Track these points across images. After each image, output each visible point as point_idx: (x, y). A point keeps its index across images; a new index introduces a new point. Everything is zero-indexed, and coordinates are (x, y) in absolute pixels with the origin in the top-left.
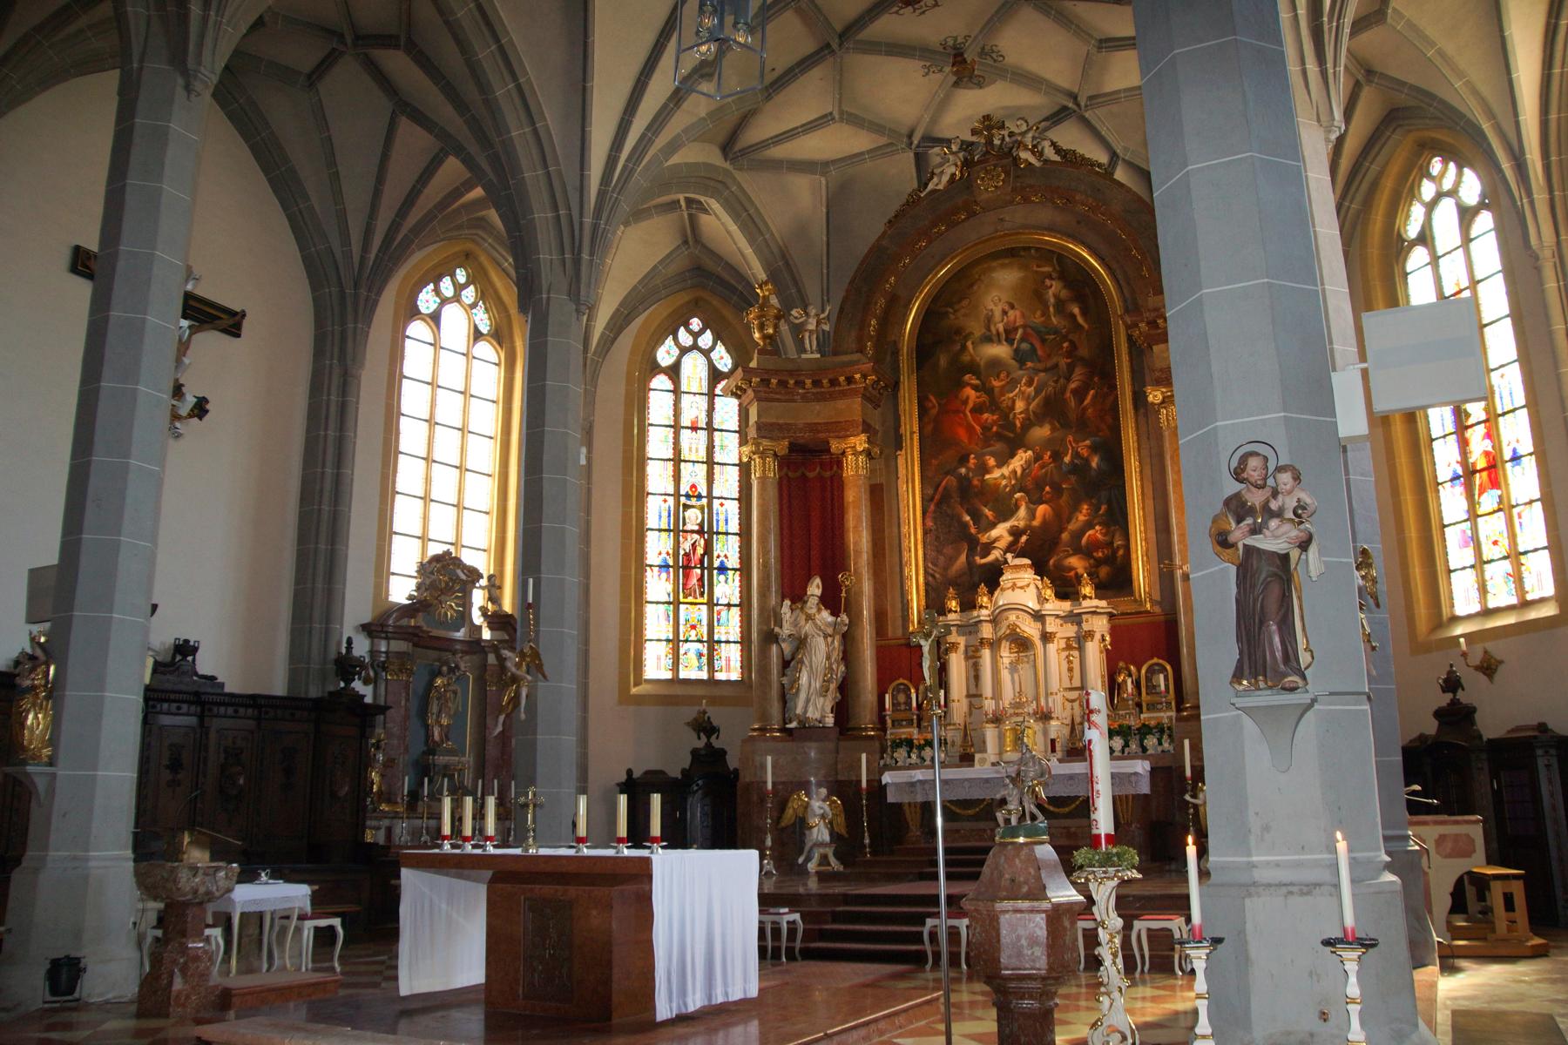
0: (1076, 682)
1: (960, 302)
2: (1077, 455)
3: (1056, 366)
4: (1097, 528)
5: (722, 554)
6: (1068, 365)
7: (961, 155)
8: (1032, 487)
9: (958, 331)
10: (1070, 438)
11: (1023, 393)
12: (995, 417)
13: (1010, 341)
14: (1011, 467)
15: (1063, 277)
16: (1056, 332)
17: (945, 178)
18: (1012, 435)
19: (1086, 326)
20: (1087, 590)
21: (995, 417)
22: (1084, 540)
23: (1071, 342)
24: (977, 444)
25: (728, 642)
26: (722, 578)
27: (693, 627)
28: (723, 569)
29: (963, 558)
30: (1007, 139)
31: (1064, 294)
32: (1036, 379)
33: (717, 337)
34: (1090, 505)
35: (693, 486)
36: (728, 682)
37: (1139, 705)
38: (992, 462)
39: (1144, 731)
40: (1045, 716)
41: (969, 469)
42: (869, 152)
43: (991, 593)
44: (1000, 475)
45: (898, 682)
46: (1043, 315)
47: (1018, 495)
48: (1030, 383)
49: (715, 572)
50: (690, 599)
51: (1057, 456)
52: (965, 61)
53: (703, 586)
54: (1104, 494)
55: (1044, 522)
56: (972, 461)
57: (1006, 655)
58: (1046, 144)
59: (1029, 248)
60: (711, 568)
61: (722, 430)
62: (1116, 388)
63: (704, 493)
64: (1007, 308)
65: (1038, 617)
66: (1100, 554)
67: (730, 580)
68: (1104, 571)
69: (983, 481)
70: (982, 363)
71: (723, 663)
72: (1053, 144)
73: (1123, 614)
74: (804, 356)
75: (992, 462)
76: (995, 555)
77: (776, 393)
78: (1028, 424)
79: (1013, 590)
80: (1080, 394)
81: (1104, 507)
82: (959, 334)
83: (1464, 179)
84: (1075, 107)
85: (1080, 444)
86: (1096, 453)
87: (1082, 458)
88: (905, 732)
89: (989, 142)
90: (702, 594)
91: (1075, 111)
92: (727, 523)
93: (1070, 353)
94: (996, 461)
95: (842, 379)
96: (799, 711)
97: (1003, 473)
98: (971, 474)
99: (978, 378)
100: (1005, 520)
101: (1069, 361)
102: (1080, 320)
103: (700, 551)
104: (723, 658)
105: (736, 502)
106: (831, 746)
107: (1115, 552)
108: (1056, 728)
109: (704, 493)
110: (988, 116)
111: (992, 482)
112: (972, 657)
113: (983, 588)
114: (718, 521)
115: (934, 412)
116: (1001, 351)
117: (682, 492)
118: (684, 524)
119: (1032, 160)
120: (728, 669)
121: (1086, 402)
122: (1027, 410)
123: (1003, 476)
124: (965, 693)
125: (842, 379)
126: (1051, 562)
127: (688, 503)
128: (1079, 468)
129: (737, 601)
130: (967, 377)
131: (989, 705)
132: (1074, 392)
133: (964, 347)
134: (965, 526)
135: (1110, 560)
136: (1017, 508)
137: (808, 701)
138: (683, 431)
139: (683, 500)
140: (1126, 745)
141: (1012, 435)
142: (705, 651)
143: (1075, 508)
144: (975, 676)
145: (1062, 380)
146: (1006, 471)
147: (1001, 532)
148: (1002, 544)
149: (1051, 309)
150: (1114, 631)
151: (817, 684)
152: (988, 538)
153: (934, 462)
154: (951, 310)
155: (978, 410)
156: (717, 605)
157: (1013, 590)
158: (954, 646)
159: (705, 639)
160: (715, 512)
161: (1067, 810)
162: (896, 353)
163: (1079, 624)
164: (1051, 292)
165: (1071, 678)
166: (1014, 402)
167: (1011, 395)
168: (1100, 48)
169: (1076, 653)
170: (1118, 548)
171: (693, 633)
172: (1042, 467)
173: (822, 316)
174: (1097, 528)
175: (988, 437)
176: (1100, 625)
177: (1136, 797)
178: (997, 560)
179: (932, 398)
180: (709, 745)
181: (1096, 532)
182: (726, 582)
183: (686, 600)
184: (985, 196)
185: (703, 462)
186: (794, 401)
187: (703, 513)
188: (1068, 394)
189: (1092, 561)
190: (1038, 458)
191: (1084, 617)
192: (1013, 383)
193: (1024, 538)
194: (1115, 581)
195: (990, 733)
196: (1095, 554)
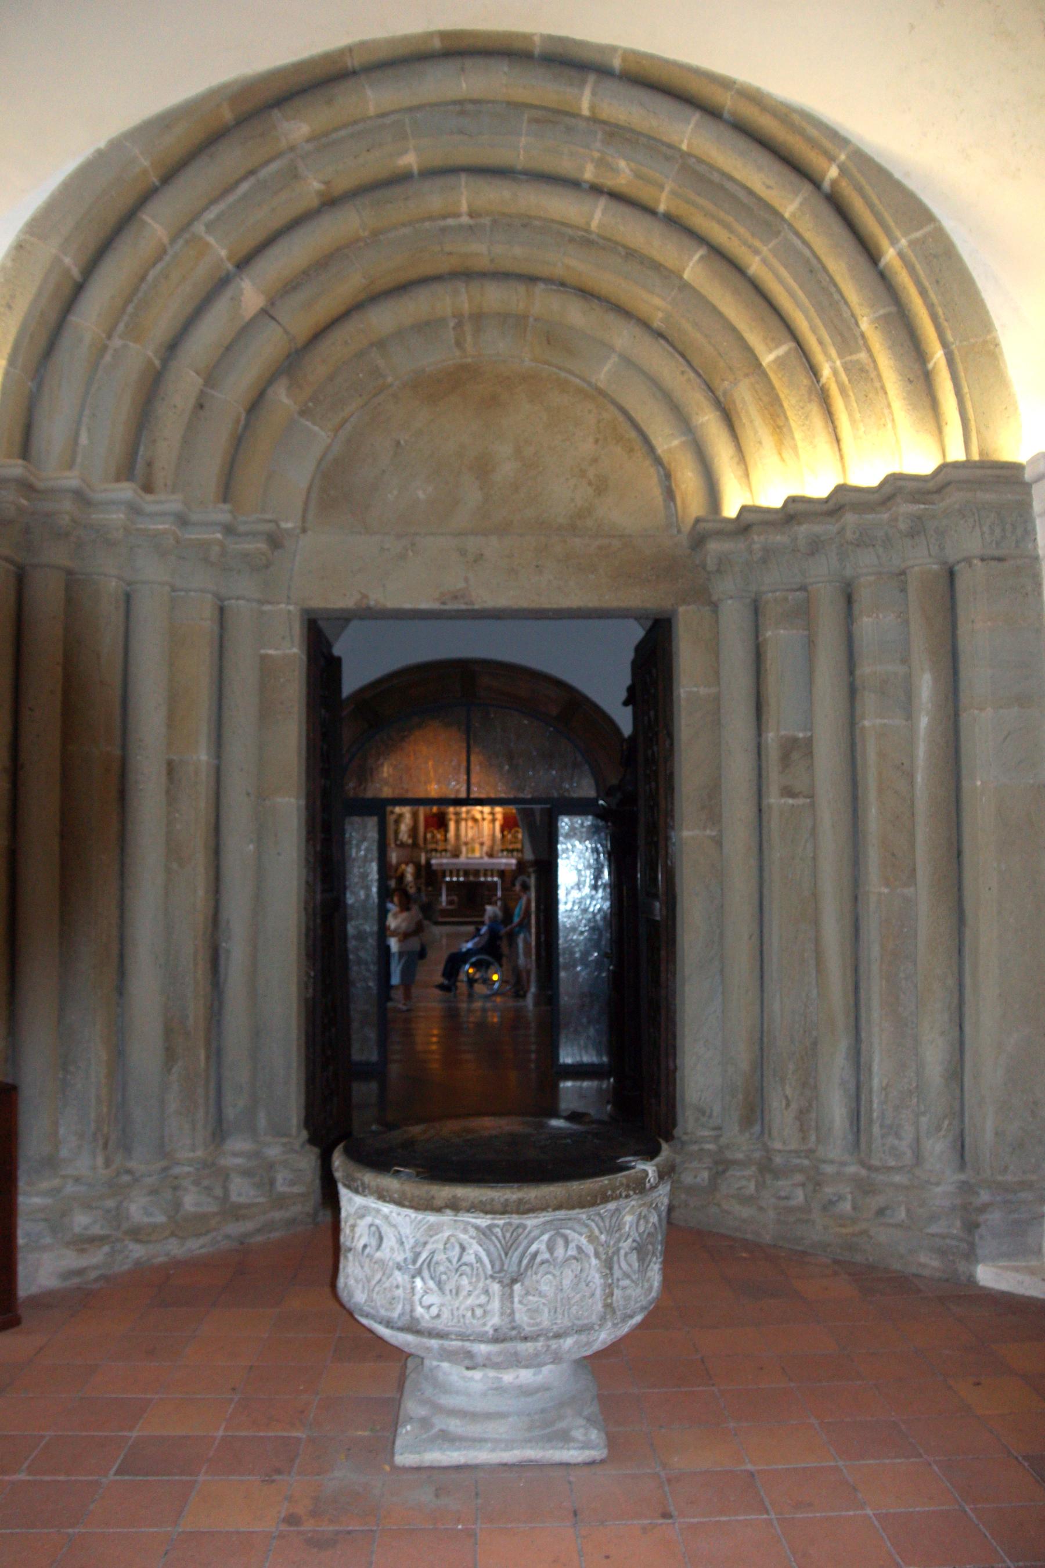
0: (491, 832)
39: (512, 851)
40: (482, 844)
57: (470, 823)
88: (433, 846)
108: (485, 848)
112: (458, 822)
131: (463, 839)
144: (457, 829)
158: (450, 820)
195: (464, 849)
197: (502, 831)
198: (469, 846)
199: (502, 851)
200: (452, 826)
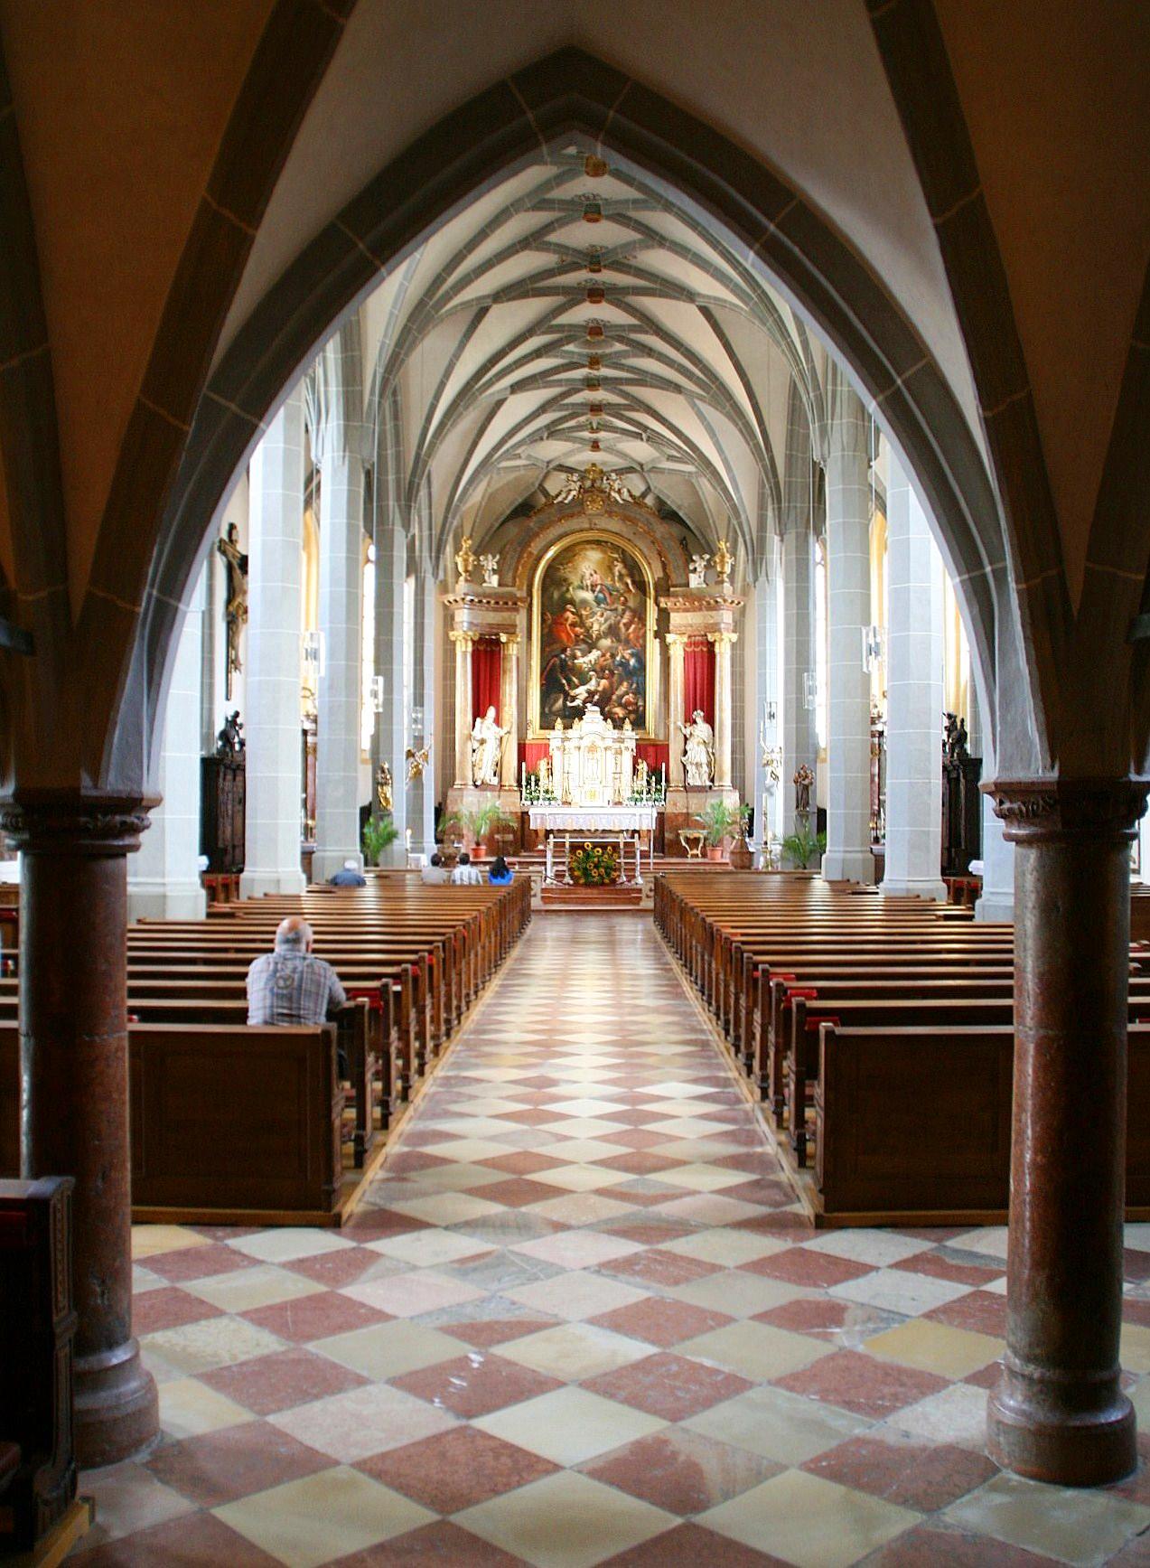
1: (570, 562)
3: (616, 609)
7: (579, 483)
8: (600, 671)
9: (565, 580)
10: (620, 648)
13: (593, 591)
15: (624, 562)
16: (618, 591)
17: (570, 497)
20: (627, 726)
22: (624, 700)
29: (561, 701)
31: (624, 571)
38: (579, 654)
42: (524, 466)
44: (585, 661)
47: (592, 673)
51: (613, 656)
54: (635, 679)
55: (604, 689)
56: (568, 652)
58: (625, 490)
59: (606, 542)
68: (632, 716)
70: (577, 600)
72: (629, 491)
76: (578, 702)
78: (599, 638)
80: (627, 626)
81: (634, 686)
82: (564, 582)
84: (639, 469)
93: (624, 604)
95: (510, 603)
97: (585, 661)
99: (575, 606)
100: (583, 683)
102: (631, 587)
107: (638, 708)
115: (549, 622)
116: (588, 596)
119: (618, 498)
122: (599, 630)
125: (510, 603)
128: (624, 664)
130: (569, 606)
132: (625, 624)
133: (568, 590)
135: (635, 711)
143: (621, 683)
146: (586, 659)
147: (581, 692)
150: (638, 746)
153: (547, 649)
155: (573, 625)
164: (617, 569)
168: (668, 459)
175: (577, 641)
176: (632, 745)
181: (630, 697)
184: (590, 512)
188: (621, 625)
190: (603, 655)
192: (594, 614)
193: (596, 697)
194: (639, 723)
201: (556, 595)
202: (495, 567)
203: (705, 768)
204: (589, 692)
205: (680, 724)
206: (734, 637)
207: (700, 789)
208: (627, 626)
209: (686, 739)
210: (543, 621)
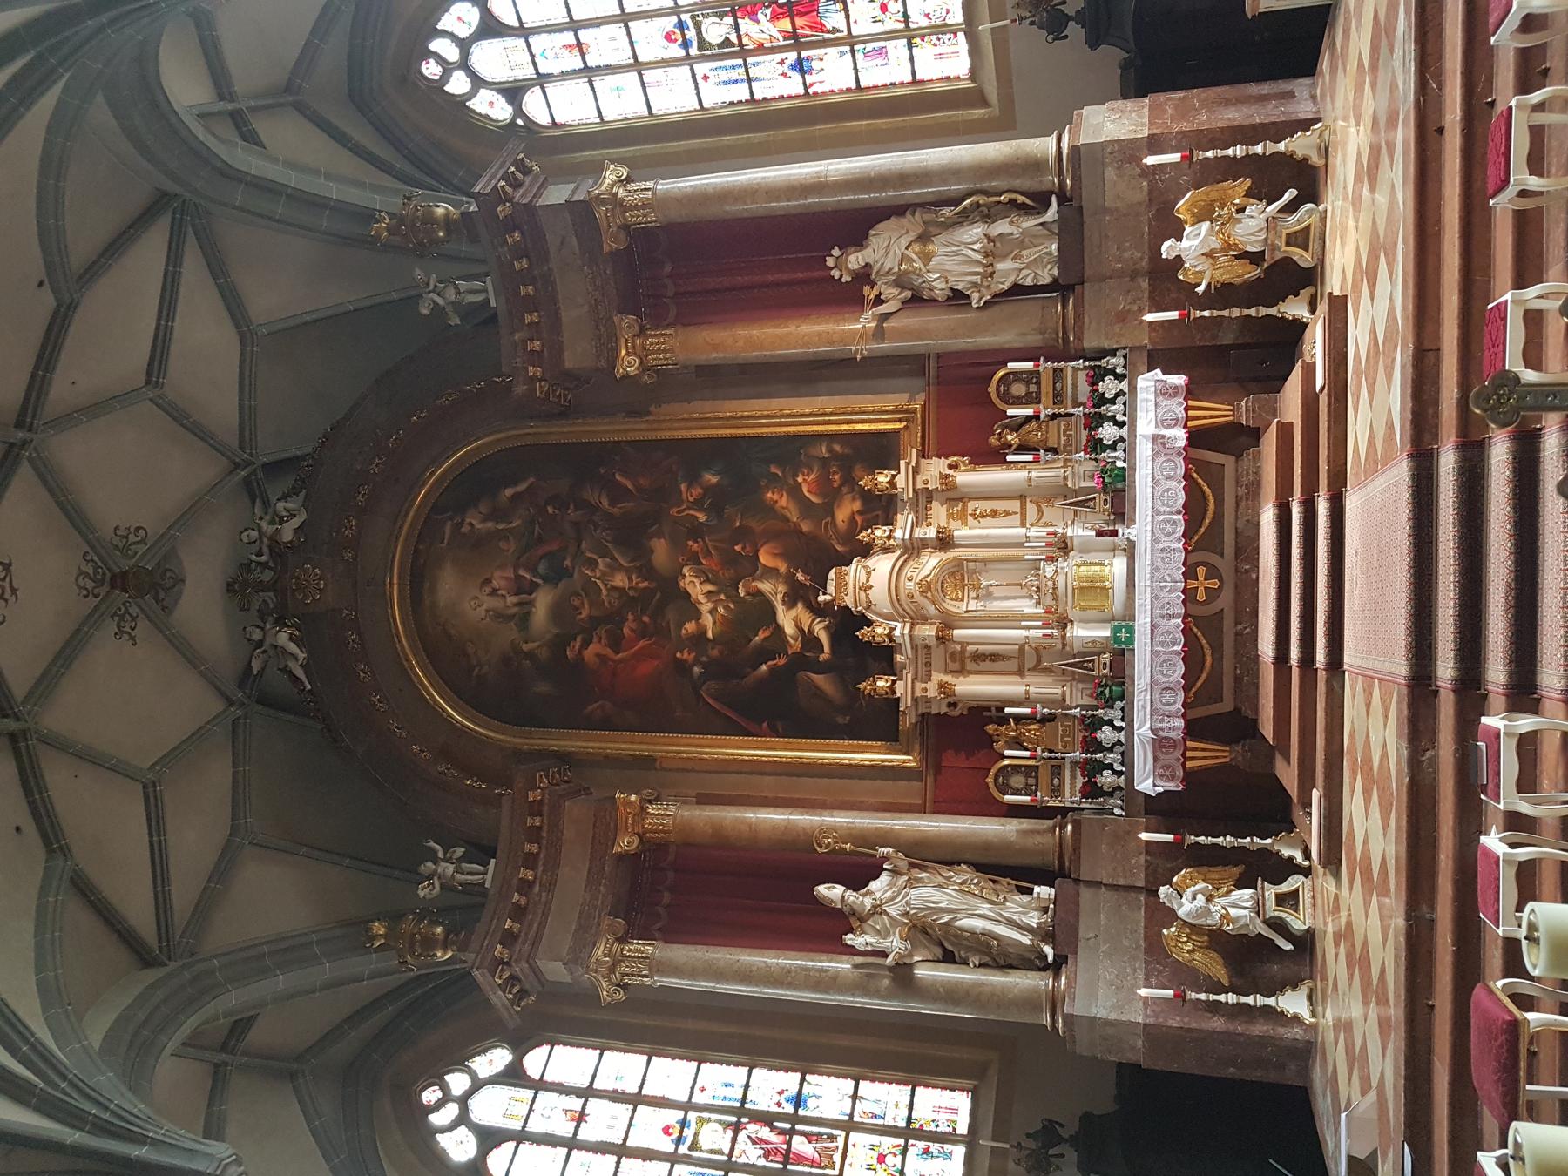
0: (1014, 505)
2: (698, 504)
4: (800, 479)
5: (777, 1098)
6: (576, 509)
10: (674, 511)
11: (604, 574)
12: (630, 617)
13: (534, 587)
14: (702, 599)
17: (293, 647)
18: (658, 595)
19: (532, 480)
20: (883, 478)
21: (630, 617)
22: (814, 499)
23: (547, 503)
24: (664, 648)
25: (911, 1107)
26: (811, 1103)
27: (881, 1159)
28: (798, 1101)
29: (818, 679)
30: (263, 558)
31: (484, 508)
32: (589, 555)
33: (460, 1064)
34: (768, 488)
35: (666, 1131)
36: (973, 1113)
37: (1054, 417)
38: (690, 627)
40: (1063, 547)
41: (696, 662)
43: (870, 623)
45: (991, 785)
46: (506, 538)
47: (742, 592)
48: (592, 564)
49: (801, 1112)
50: (837, 1158)
51: (696, 531)
52: (124, 574)
53: (819, 1135)
55: (783, 555)
56: (685, 655)
58: (281, 506)
59: (416, 550)
60: (795, 1119)
61: (594, 1077)
62: (619, 442)
63: (681, 1114)
64: (488, 589)
65: (913, 549)
66: (836, 477)
67: (817, 1091)
69: (715, 641)
71: (942, 1118)
72: (284, 498)
73: (923, 445)
74: (487, 885)
75: (690, 627)
76: (820, 630)
77: (530, 926)
78: (647, 571)
79: (871, 587)
80: (618, 494)
81: (774, 469)
83: (449, 29)
85: (684, 496)
86: (700, 476)
87: (704, 495)
89: (261, 587)
90: (832, 1138)
91: (254, 472)
92: (731, 1085)
94: (690, 621)
96: (1026, 940)
98: (704, 659)
100: (774, 613)
101: (572, 507)
102: (521, 487)
103: (765, 1132)
104: (935, 1116)
105: (703, 1066)
106: (1086, 894)
107: (835, 456)
109: (681, 1114)
110: (229, 584)
111: (718, 629)
113: (864, 633)
114: (725, 1098)
116: (543, 602)
117: (670, 1148)
118: (720, 1152)
119: (296, 522)
120: (954, 1111)
121: (630, 486)
122: (628, 571)
123: (712, 612)
124: (1017, 679)
126: (839, 548)
127: (688, 1142)
128: (716, 501)
129: (850, 1083)
132: (613, 503)
133: (530, 655)
134: (772, 670)
136: (759, 593)
137: (1011, 923)
138: (581, 1136)
139: (683, 1149)
140: (1113, 419)
141: (658, 595)
142: (922, 1145)
143: (770, 509)
145: (596, 518)
146: (705, 607)
147: (788, 620)
148: (806, 618)
149: (501, 527)
151: (985, 908)
152: (796, 640)
154: (477, 670)
155: (616, 643)
156: (851, 1115)
157: (871, 587)
159: (901, 1141)
160: (711, 1102)
161: (1211, 499)
162: (520, 756)
163: (929, 495)
164: (478, 526)
165: (1007, 513)
166: (614, 588)
167: (604, 592)
169: (971, 505)
170: (830, 451)
171: (890, 1160)
172: (708, 554)
173: (441, 855)
174: (800, 479)
176: (935, 468)
177: (1190, 392)
178: (827, 628)
179: (590, 708)
180: (1073, 1141)
181: (806, 481)
182: (817, 1097)
183: (838, 1166)
185: (634, 1111)
186: (548, 903)
187: (709, 1120)
189: (845, 489)
190: (694, 560)
191: (920, 485)
192: (589, 588)
193: (800, 576)
196: (835, 485)
197: (996, 457)
198: (1072, 614)
199: (1095, 445)
200: (976, 686)
201: (543, 688)
202: (460, 851)
203: (1002, 227)
204: (790, 602)
205: (866, 320)
206: (611, 175)
207: (1071, 233)
208: (618, 494)
209: (917, 300)
210: (607, 724)
